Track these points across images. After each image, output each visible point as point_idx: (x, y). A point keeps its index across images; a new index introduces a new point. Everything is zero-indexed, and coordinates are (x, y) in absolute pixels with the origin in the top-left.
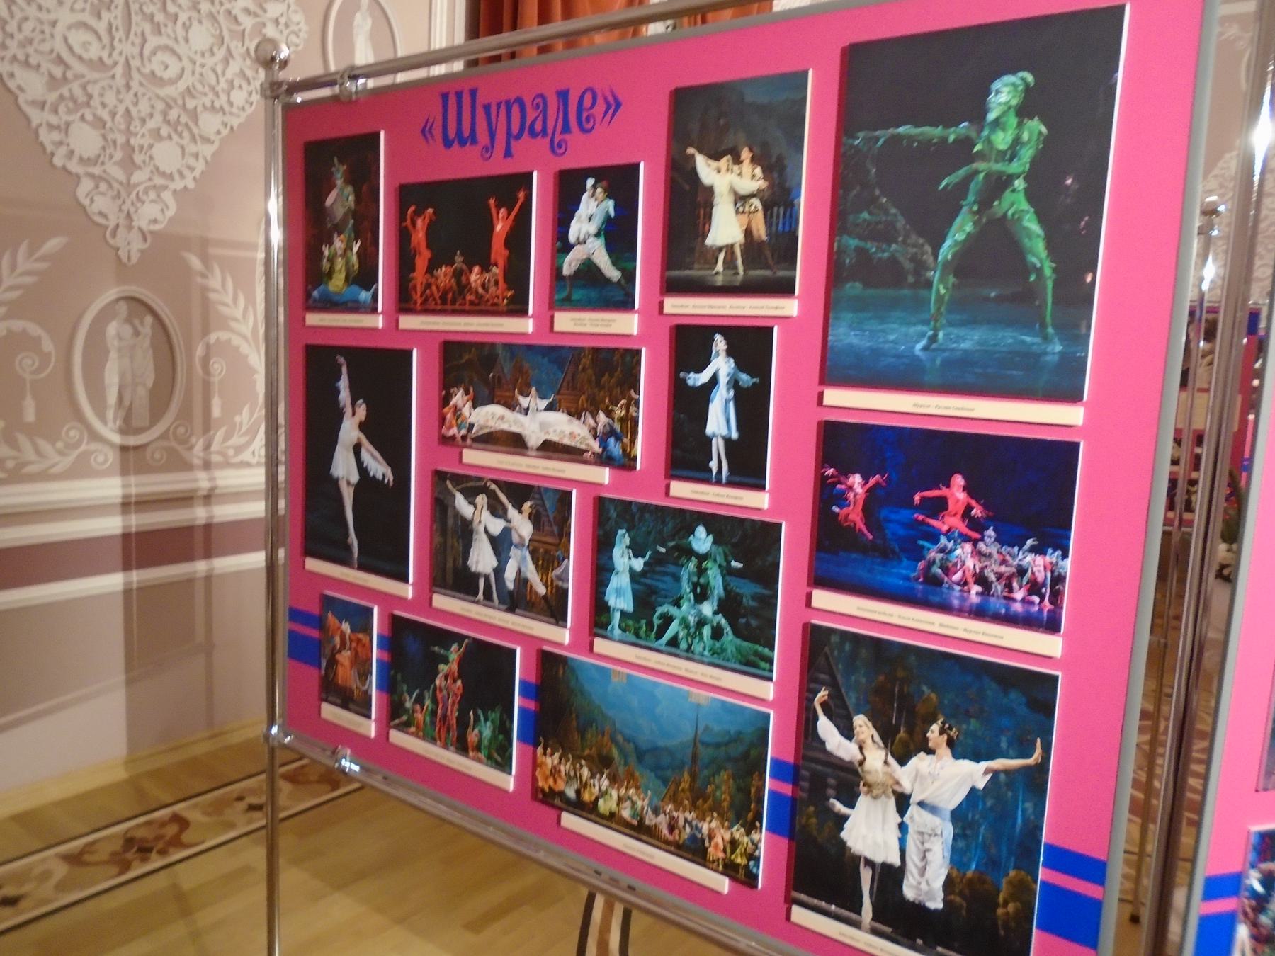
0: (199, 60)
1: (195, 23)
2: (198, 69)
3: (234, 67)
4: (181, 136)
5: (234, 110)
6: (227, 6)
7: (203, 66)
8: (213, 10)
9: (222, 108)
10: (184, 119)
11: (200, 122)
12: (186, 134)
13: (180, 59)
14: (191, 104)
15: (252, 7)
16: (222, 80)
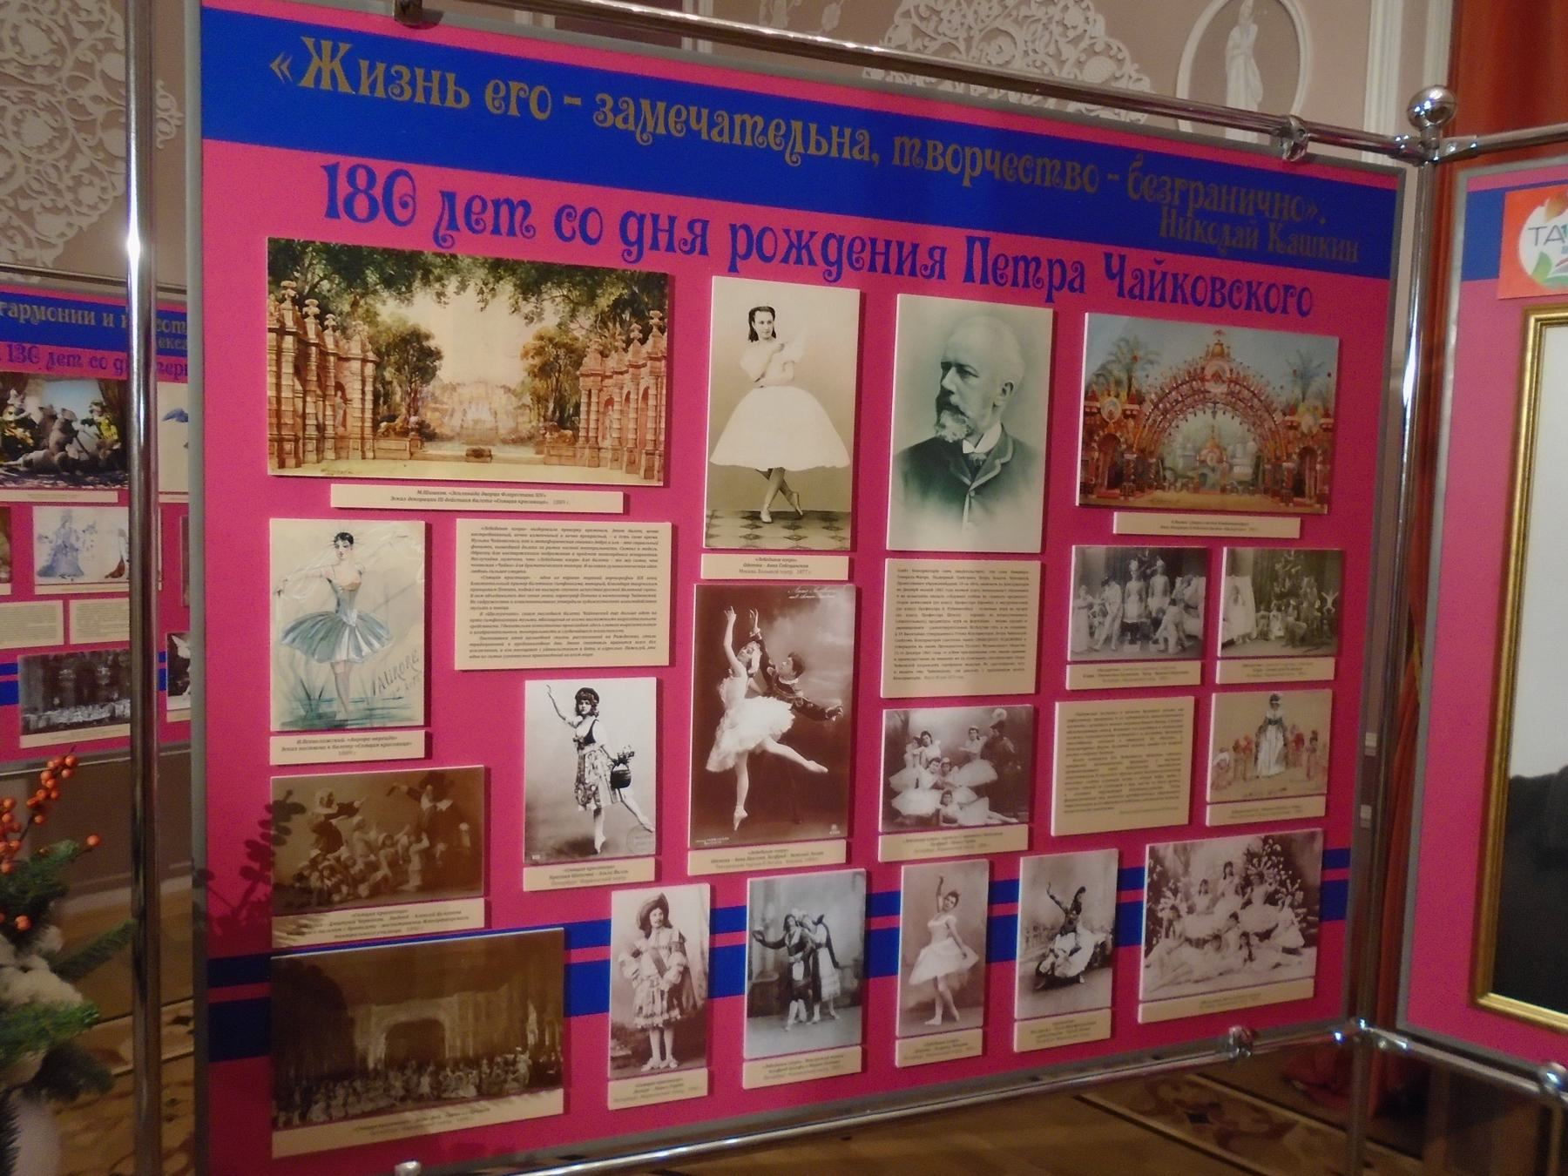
0: (35, 156)
1: (29, 116)
2: (34, 167)
3: (82, 162)
4: (11, 239)
5: (85, 210)
6: (72, 94)
7: (40, 162)
8: (53, 100)
9: (66, 209)
10: (16, 222)
11: (38, 227)
12: (19, 239)
13: (10, 156)
14: (24, 205)
15: (104, 94)
16: (66, 177)
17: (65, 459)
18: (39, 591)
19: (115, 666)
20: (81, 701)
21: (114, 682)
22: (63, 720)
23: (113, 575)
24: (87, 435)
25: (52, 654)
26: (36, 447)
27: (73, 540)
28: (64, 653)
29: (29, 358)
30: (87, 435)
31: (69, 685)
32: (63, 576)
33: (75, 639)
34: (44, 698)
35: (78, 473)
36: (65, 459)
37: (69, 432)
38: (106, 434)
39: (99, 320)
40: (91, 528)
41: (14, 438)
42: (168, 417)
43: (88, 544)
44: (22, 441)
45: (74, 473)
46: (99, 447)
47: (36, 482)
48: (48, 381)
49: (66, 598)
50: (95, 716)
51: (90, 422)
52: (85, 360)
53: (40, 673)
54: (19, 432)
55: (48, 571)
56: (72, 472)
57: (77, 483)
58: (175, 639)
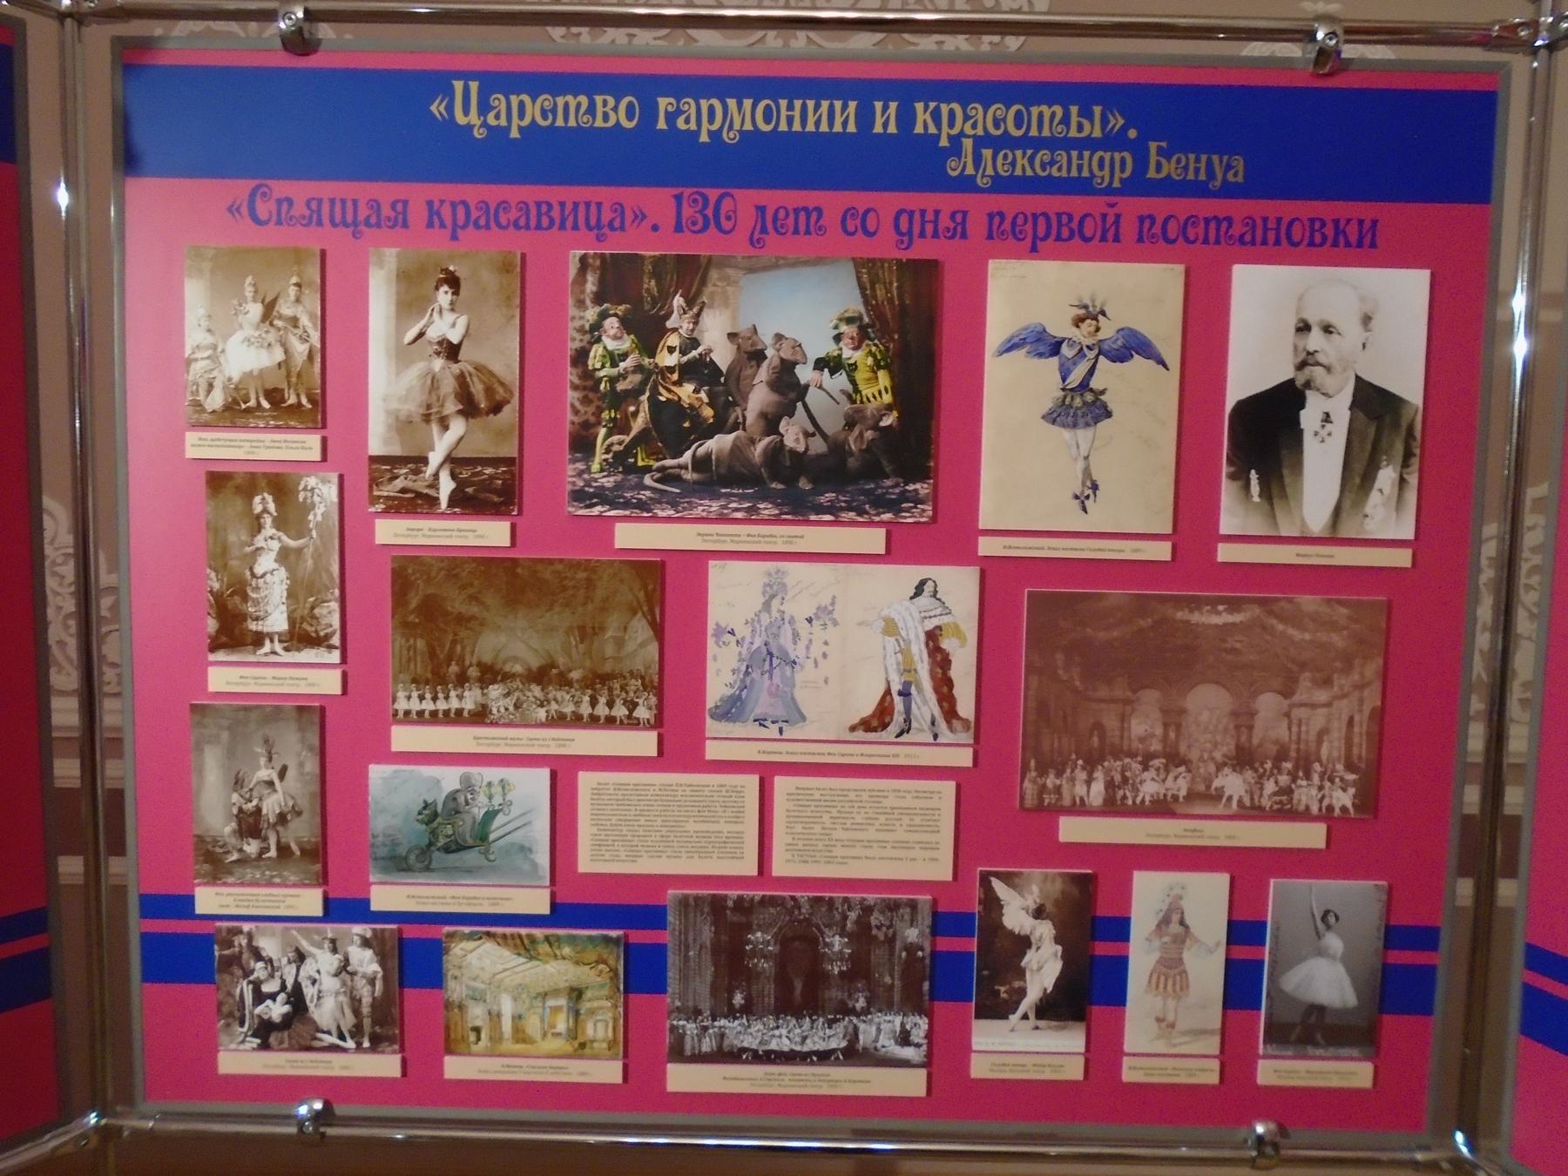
17: (777, 451)
18: (713, 751)
19: (862, 935)
20: (786, 1007)
21: (859, 971)
22: (749, 1042)
23: (866, 725)
24: (825, 395)
25: (734, 893)
26: (720, 426)
27: (786, 639)
28: (758, 894)
29: (713, 220)
30: (825, 395)
31: (765, 965)
32: (761, 722)
33: (781, 867)
34: (714, 990)
35: (804, 484)
36: (777, 451)
37: (788, 387)
38: (867, 391)
39: (865, 117)
40: (824, 614)
41: (676, 405)
42: (1010, 347)
43: (816, 650)
44: (693, 413)
45: (797, 483)
46: (850, 424)
47: (715, 506)
48: (751, 270)
49: (767, 772)
50: (815, 1044)
51: (829, 364)
52: (832, 217)
53: (707, 933)
54: (686, 392)
55: (731, 709)
56: (791, 481)
57: (798, 509)
58: (997, 885)
